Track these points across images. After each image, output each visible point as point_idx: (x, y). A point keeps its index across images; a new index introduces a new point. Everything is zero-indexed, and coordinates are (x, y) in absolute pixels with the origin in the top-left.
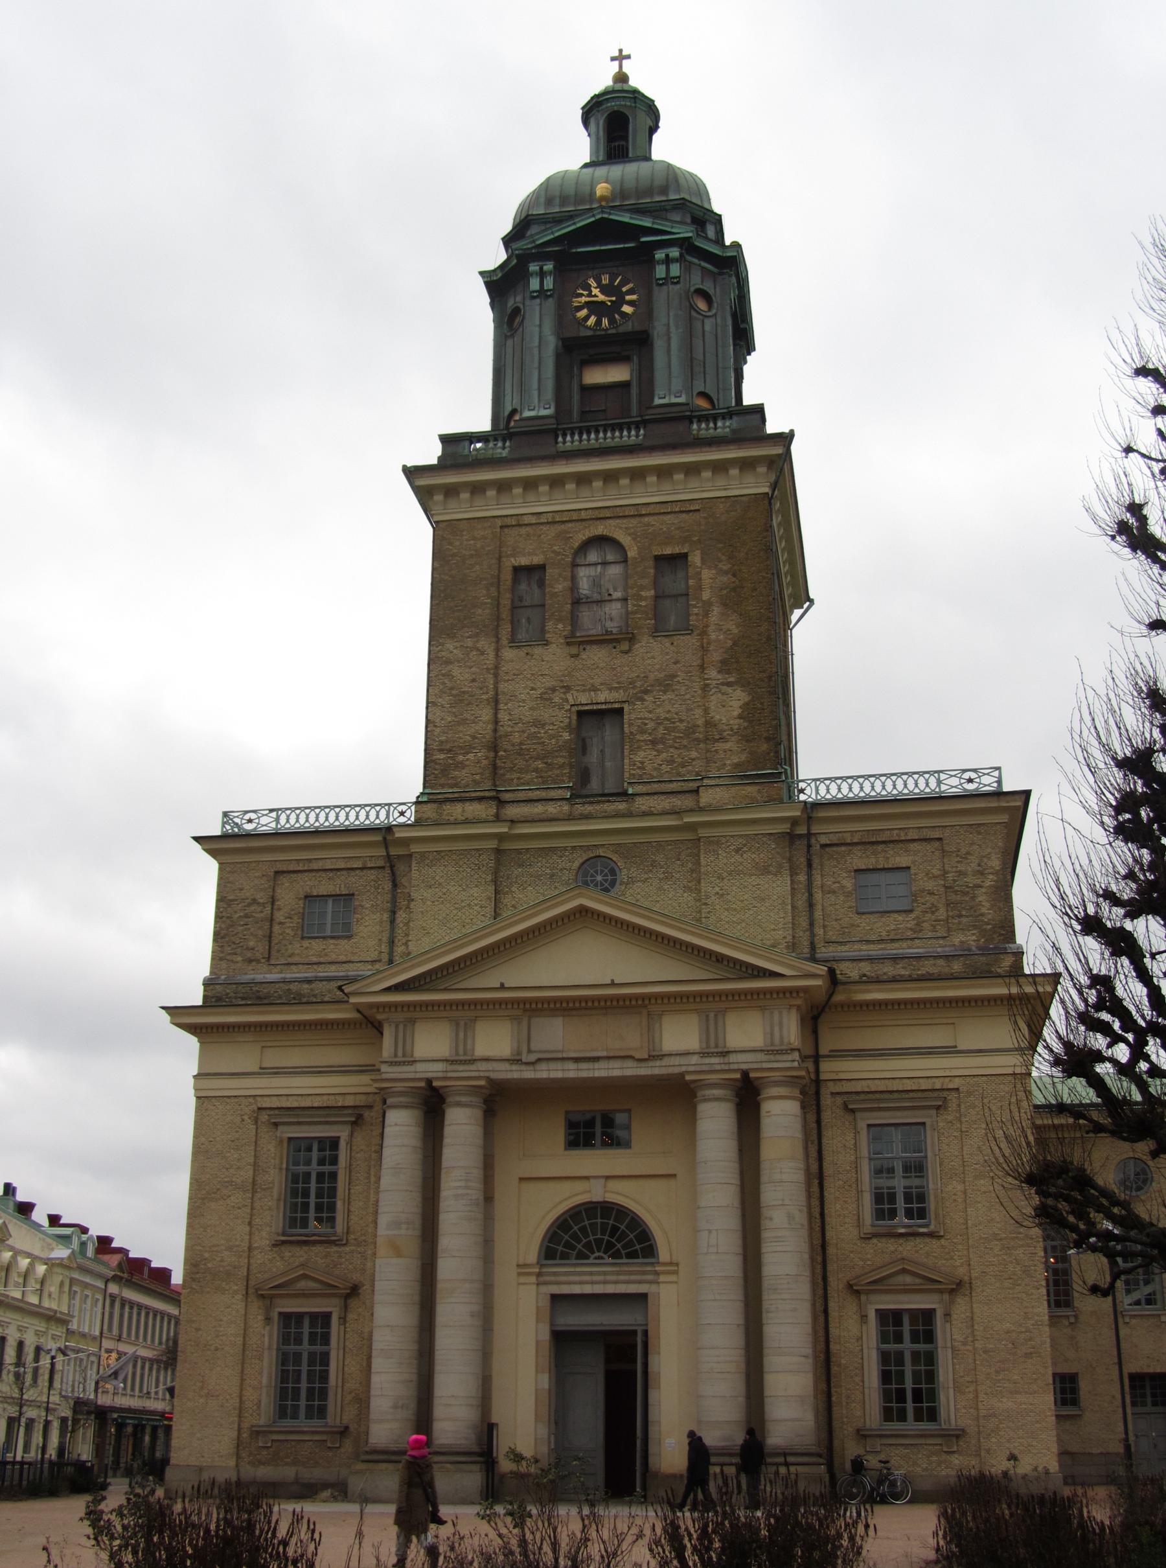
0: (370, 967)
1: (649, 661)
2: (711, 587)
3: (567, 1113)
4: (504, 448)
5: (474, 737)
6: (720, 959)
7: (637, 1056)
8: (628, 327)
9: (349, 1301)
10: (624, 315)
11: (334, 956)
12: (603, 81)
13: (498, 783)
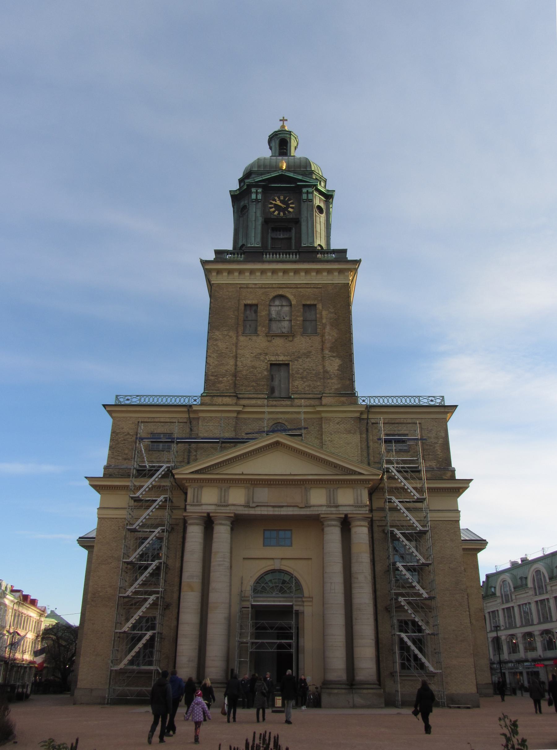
0: (179, 464)
1: (301, 345)
2: (326, 318)
3: (264, 530)
4: (241, 258)
5: (227, 371)
6: (336, 466)
7: (300, 506)
8: (291, 216)
10: (289, 212)
12: (277, 128)
13: (236, 390)
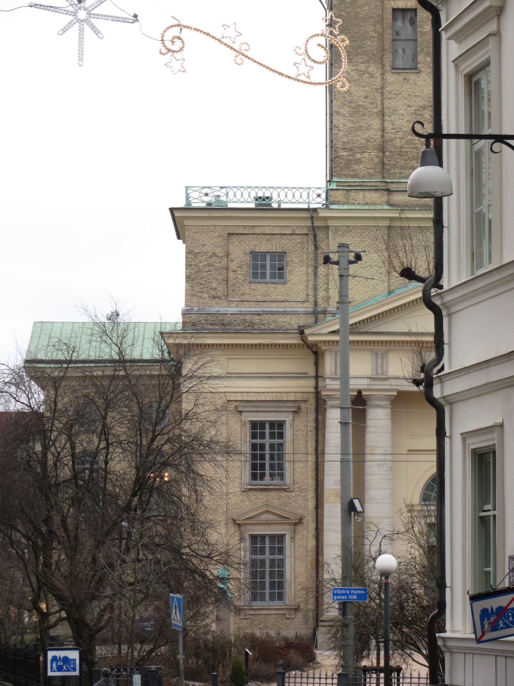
0: (301, 305)
5: (368, 141)
9: (296, 527)
11: (274, 296)
13: (385, 175)
